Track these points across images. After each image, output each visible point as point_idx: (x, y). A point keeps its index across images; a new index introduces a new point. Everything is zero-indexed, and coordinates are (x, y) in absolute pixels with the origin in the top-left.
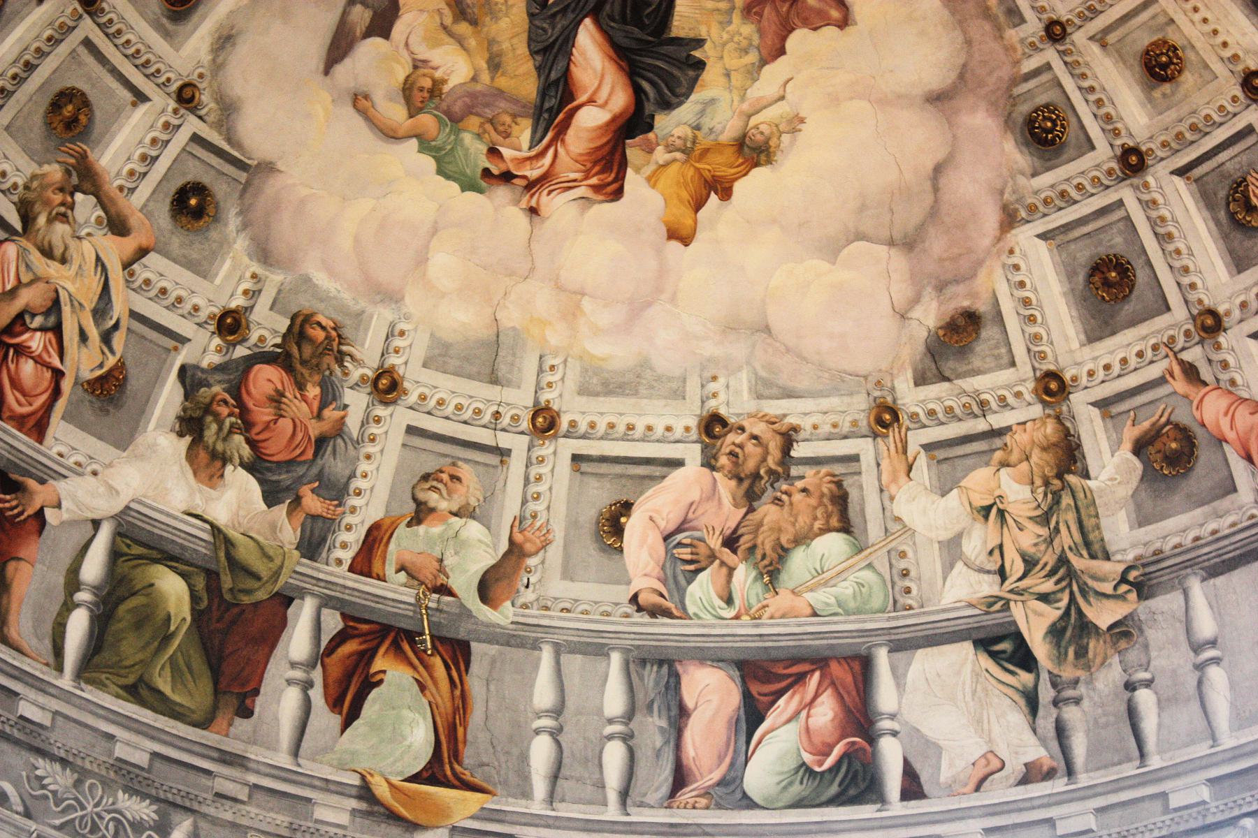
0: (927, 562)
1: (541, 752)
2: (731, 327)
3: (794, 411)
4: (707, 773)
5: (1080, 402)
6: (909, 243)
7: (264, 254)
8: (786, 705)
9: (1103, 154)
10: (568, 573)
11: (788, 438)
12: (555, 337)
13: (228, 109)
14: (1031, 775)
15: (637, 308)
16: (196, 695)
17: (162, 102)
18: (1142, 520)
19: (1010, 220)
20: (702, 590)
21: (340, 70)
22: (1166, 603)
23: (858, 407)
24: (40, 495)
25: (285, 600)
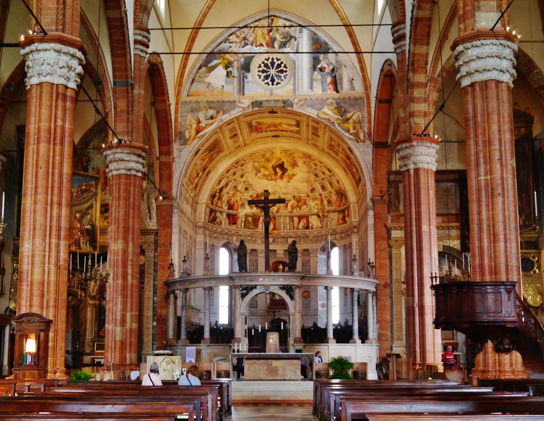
0: (313, 208)
1: (282, 226)
2: (294, 188)
3: (301, 195)
4: (296, 227)
5: (323, 196)
6: (308, 182)
7: (253, 190)
8: (302, 220)
9: (320, 178)
10: (283, 210)
11: (300, 197)
12: (280, 191)
13: (248, 182)
14: (320, 228)
15: (286, 188)
16: (253, 227)
17: (242, 183)
18: (328, 207)
19: (315, 181)
20: (295, 210)
21: (257, 176)
22: (329, 214)
23: (306, 195)
24: (238, 215)
25: (260, 217)
